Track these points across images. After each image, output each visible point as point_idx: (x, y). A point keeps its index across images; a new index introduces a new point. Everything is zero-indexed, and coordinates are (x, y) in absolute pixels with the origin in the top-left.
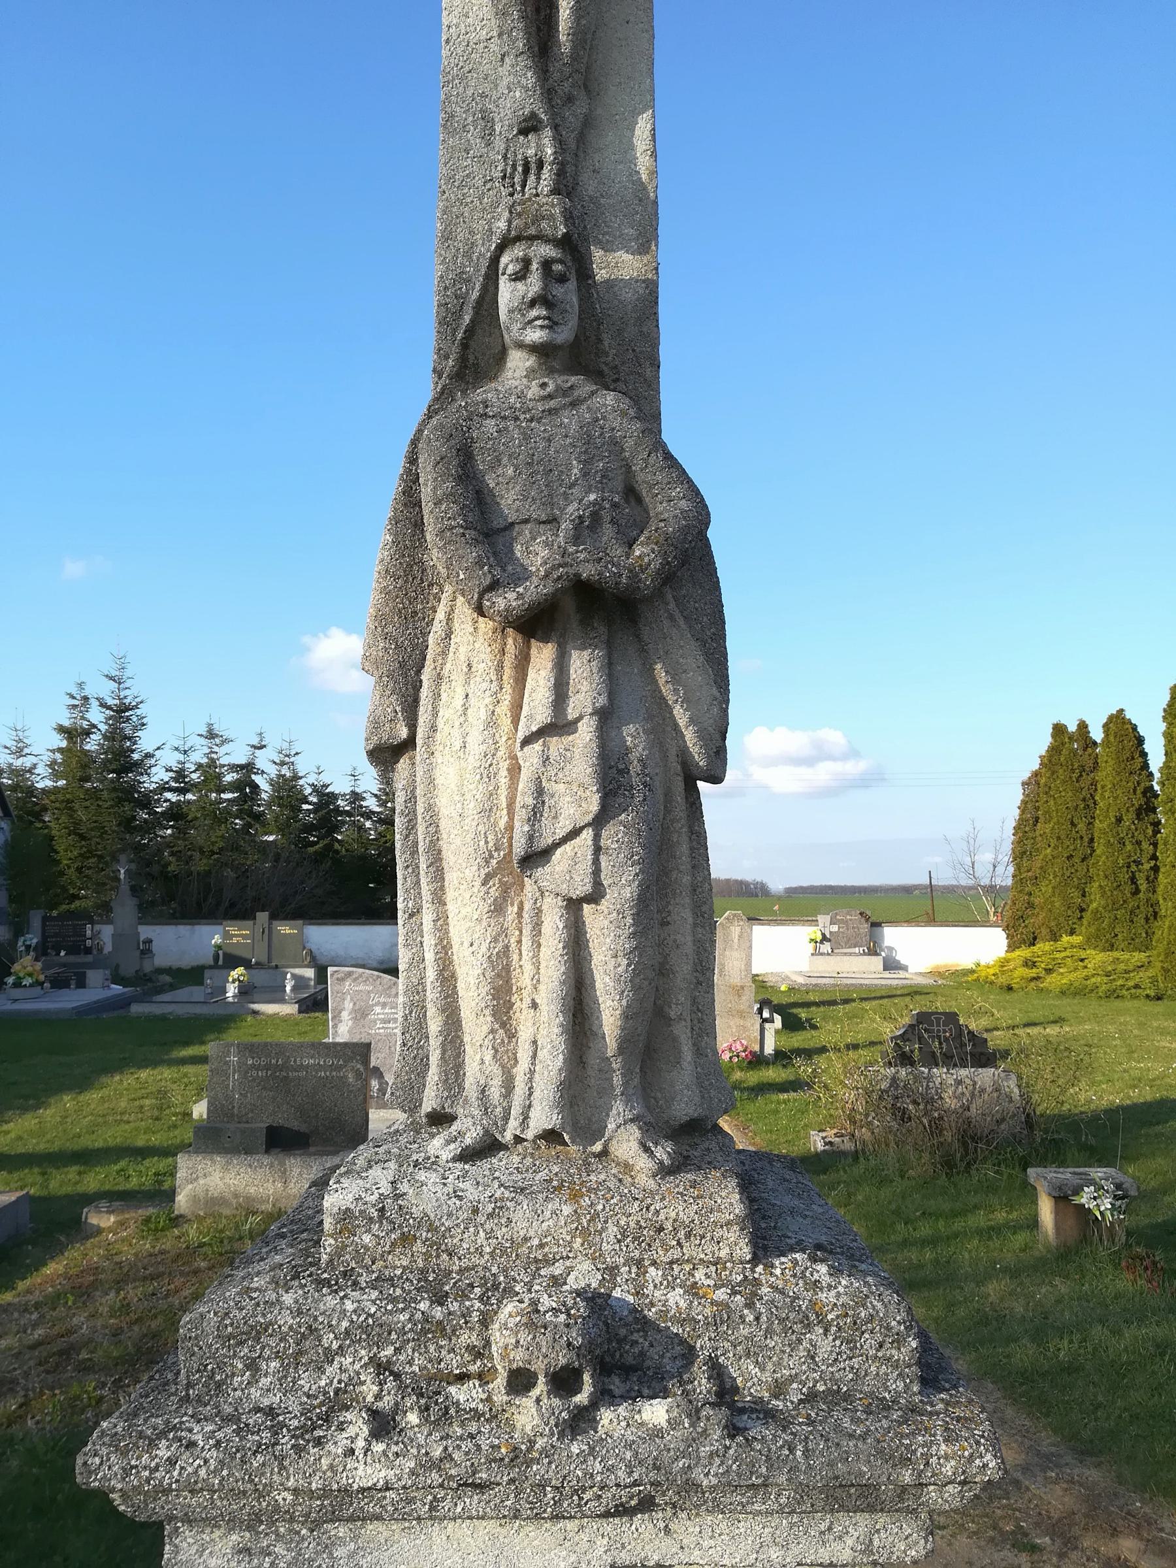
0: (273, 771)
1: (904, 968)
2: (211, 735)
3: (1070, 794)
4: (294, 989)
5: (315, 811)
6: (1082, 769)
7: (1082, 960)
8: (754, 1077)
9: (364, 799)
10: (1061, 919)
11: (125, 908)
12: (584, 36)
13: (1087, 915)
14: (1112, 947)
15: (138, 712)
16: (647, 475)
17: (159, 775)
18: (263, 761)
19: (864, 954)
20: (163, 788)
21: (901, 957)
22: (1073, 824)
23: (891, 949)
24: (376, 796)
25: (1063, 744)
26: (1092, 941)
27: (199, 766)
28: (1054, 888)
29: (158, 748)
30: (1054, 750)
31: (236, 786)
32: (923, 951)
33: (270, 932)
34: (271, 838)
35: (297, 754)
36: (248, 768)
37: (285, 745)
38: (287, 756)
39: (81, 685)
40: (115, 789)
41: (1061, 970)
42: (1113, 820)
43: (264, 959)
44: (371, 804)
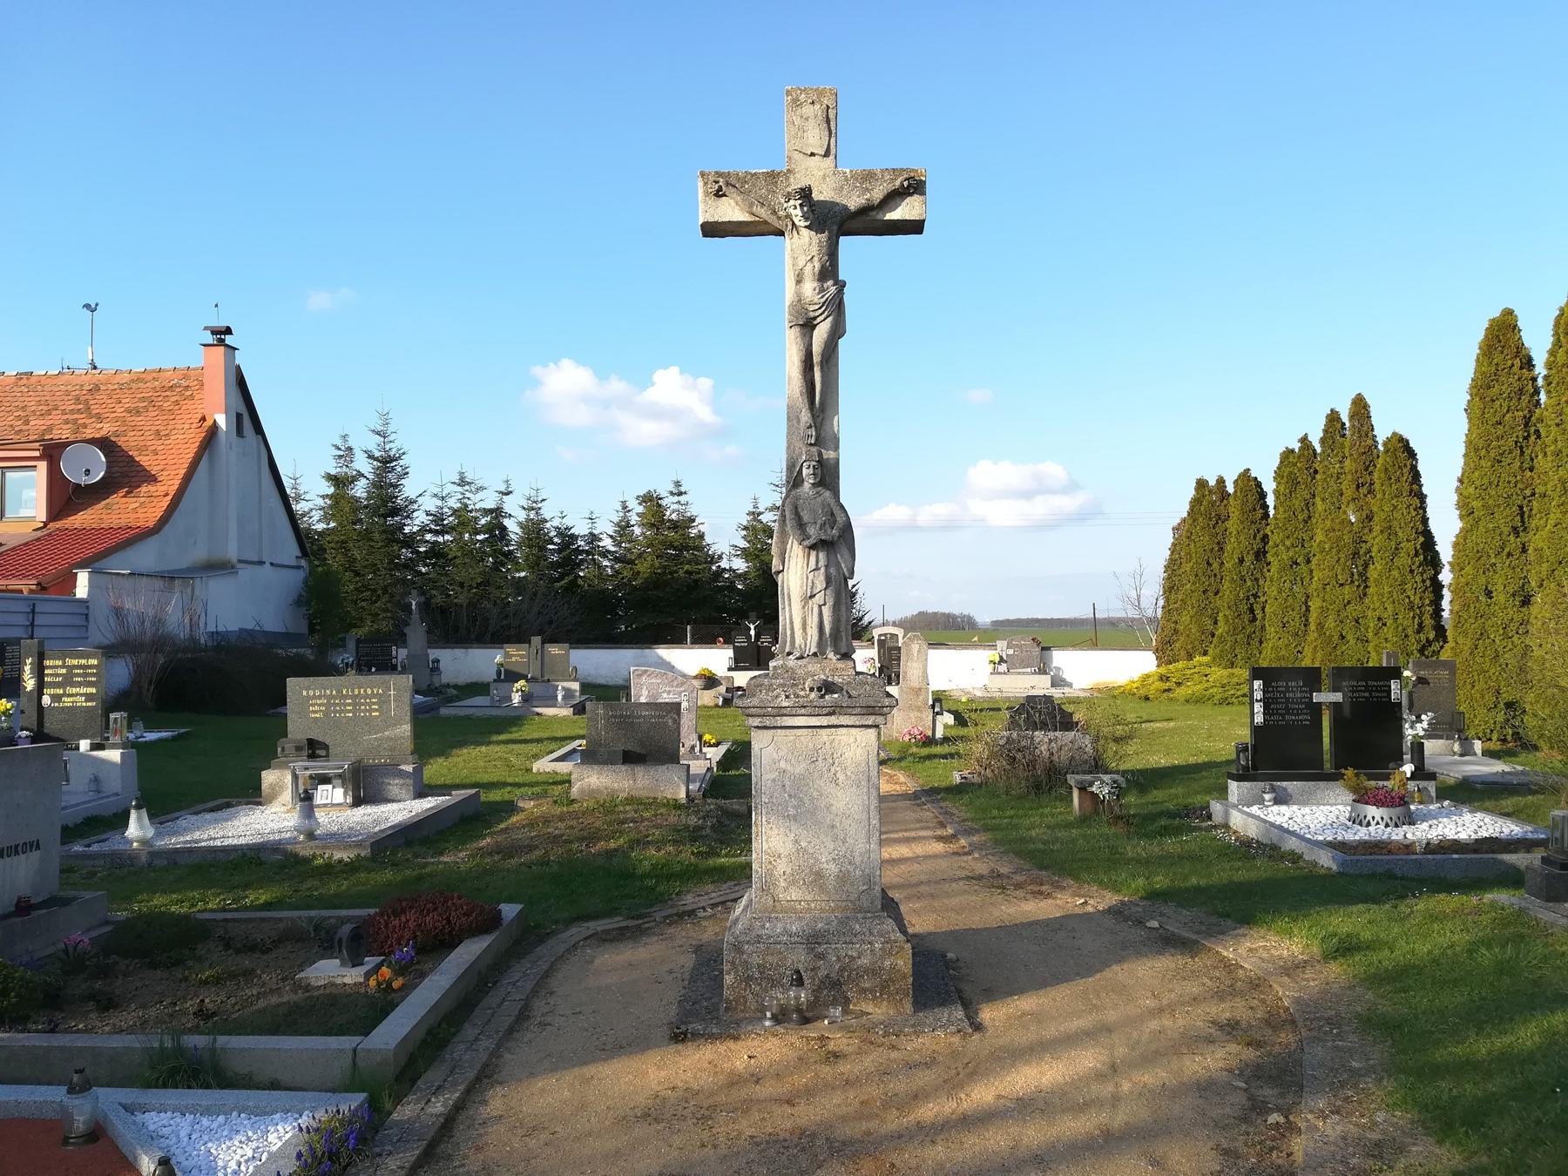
0: (522, 516)
1: (1070, 685)
2: (462, 482)
4: (564, 697)
5: (559, 551)
6: (1219, 516)
8: (925, 751)
11: (417, 632)
14: (1232, 665)
17: (420, 518)
20: (424, 529)
21: (1067, 676)
23: (1058, 669)
27: (455, 512)
30: (1196, 503)
31: (489, 529)
32: (1084, 671)
33: (542, 653)
34: (523, 574)
36: (497, 512)
37: (533, 493)
39: (344, 437)
40: (384, 531)
43: (538, 674)
44: (607, 543)
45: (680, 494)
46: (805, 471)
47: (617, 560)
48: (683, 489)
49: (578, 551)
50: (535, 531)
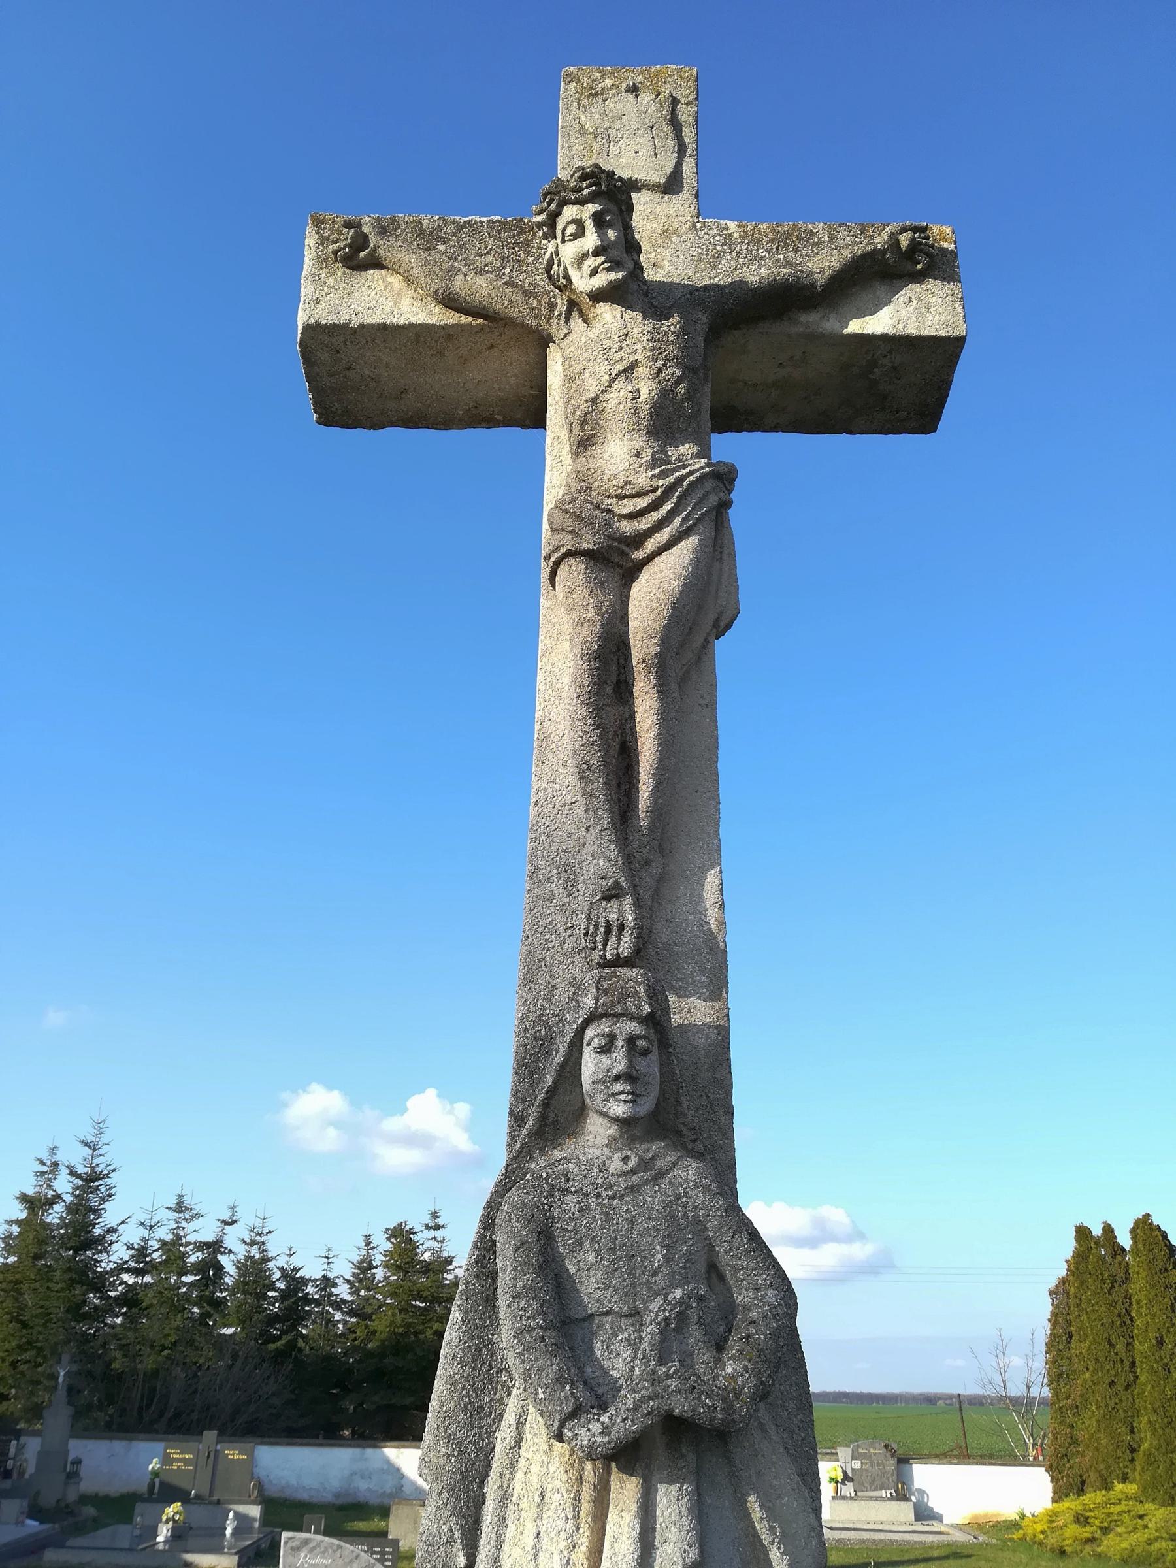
0: (241, 1251)
1: (938, 1518)
2: (180, 1207)
3: (1104, 1308)
4: (236, 1532)
7: (1141, 1517)
9: (335, 1285)
10: (1111, 1461)
11: (59, 1416)
12: (659, 811)
13: (1140, 1456)
15: (108, 1181)
16: (731, 1255)
17: (119, 1253)
18: (234, 1239)
19: (892, 1499)
20: (121, 1268)
21: (935, 1503)
22: (1111, 1345)
23: (922, 1492)
24: (348, 1282)
25: (1090, 1249)
26: (1149, 1492)
27: (164, 1243)
28: (1098, 1421)
29: (123, 1222)
33: (215, 1457)
34: (229, 1331)
35: (270, 1232)
36: (215, 1247)
37: (258, 1222)
38: (259, 1234)
39: (53, 1150)
40: (69, 1269)
41: (1119, 1530)
42: (1154, 1341)
43: (205, 1491)
44: (343, 1291)
45: (437, 1227)
46: (591, 1065)
47: (351, 1313)
48: (441, 1222)
49: (307, 1300)
50: (255, 1271)
